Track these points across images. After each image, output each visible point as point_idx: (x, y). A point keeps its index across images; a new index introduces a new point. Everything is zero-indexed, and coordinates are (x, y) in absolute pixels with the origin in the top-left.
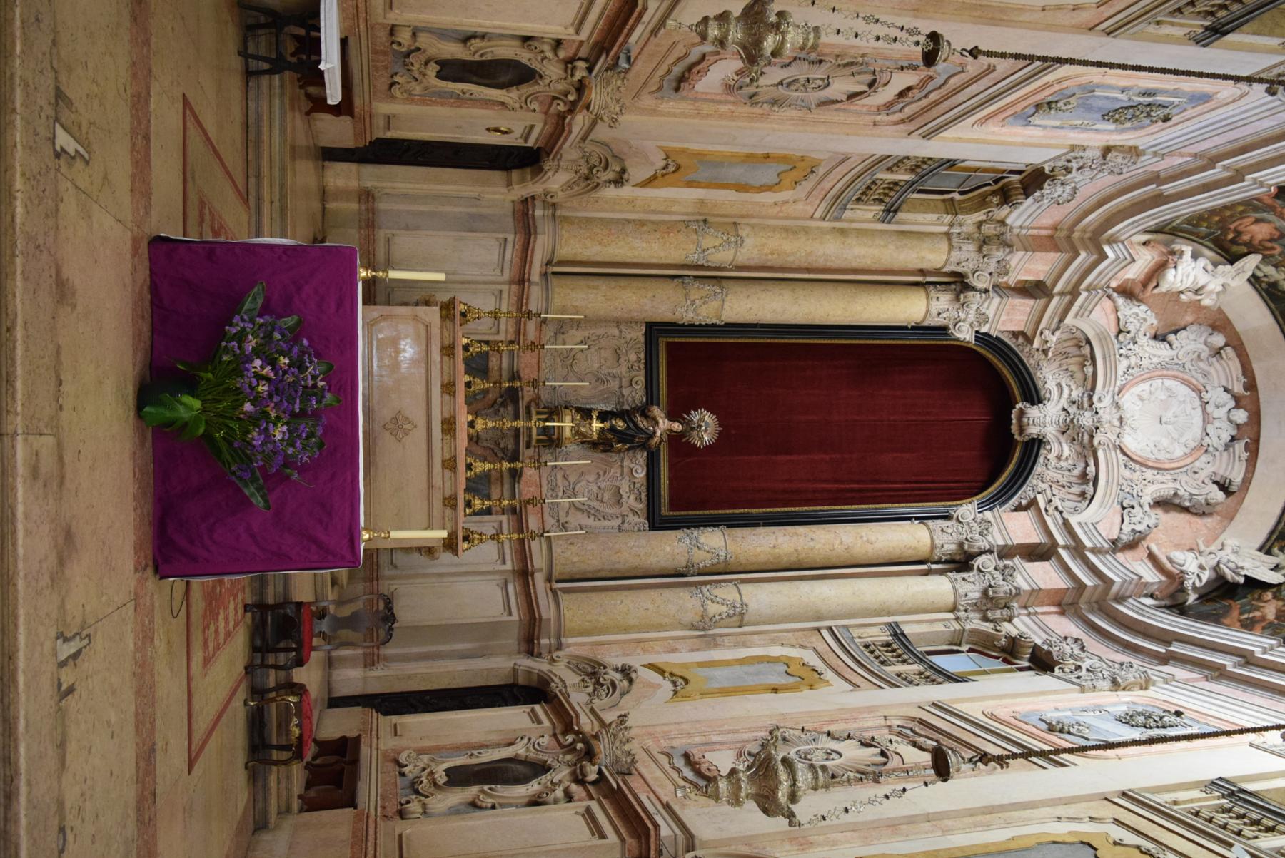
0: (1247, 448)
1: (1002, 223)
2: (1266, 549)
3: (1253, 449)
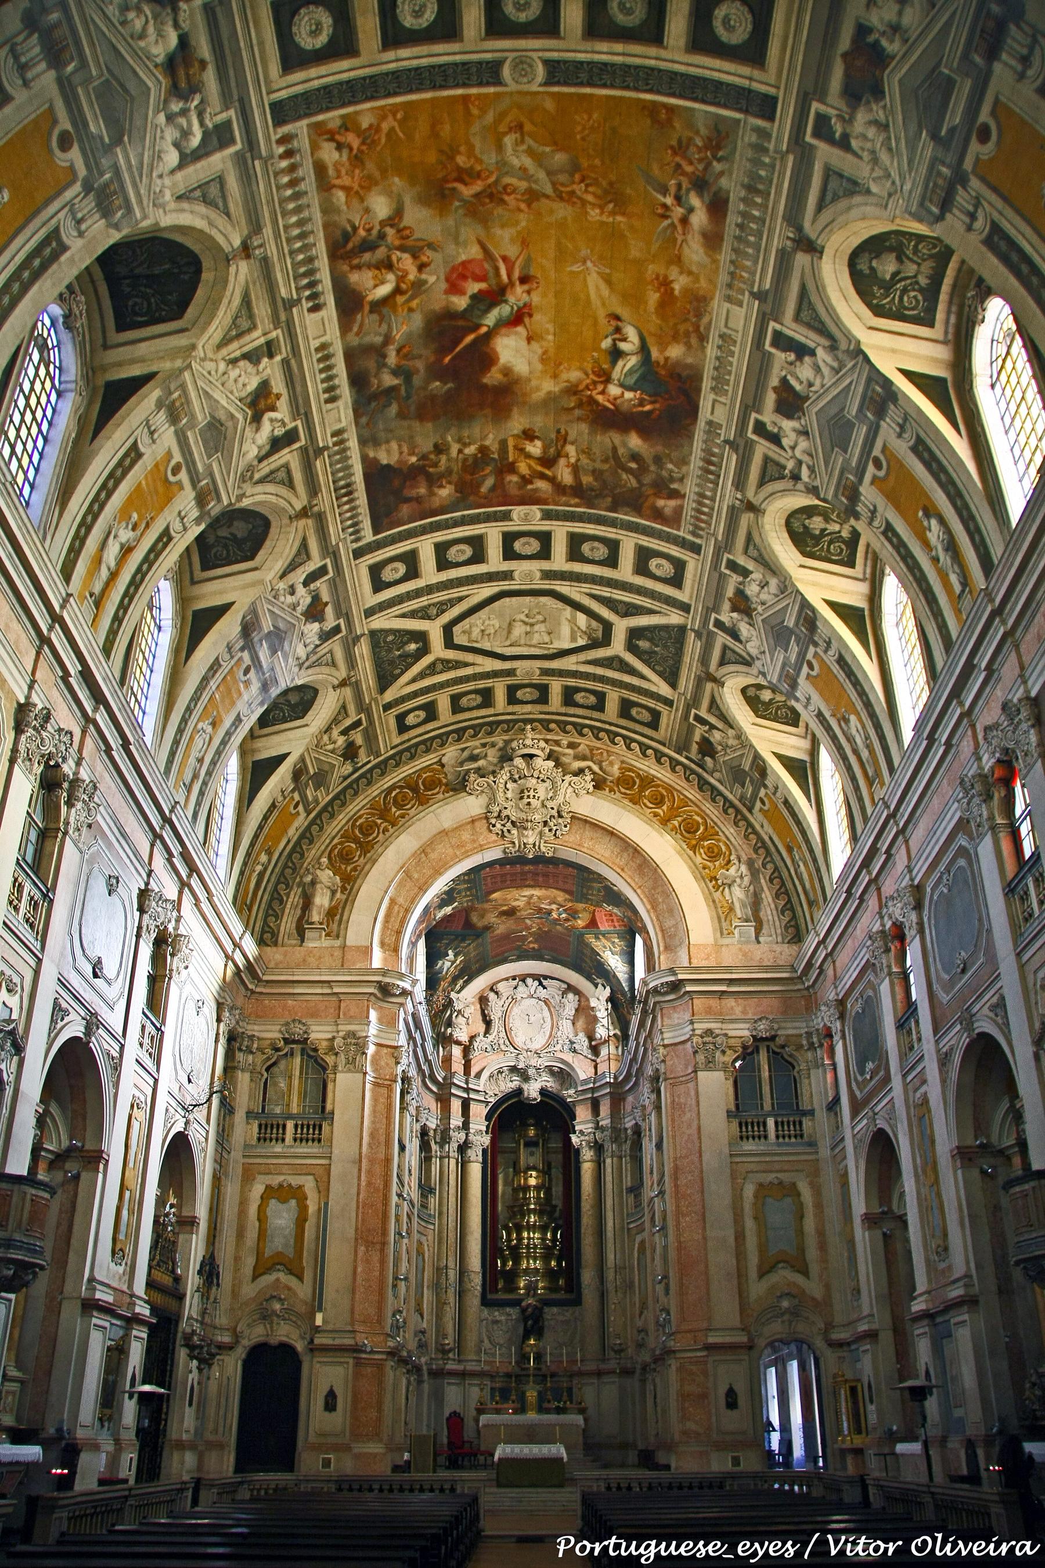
0: (546, 977)
1: (435, 1130)
2: (596, 986)
3: (546, 977)
